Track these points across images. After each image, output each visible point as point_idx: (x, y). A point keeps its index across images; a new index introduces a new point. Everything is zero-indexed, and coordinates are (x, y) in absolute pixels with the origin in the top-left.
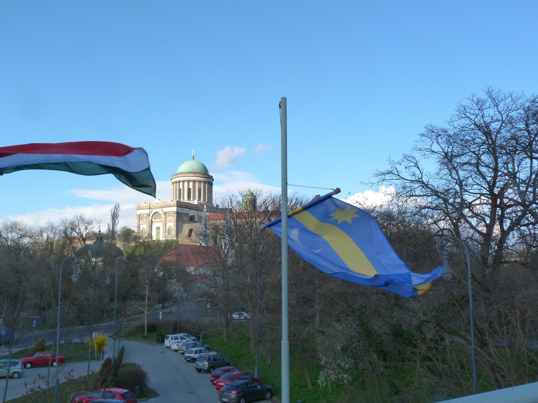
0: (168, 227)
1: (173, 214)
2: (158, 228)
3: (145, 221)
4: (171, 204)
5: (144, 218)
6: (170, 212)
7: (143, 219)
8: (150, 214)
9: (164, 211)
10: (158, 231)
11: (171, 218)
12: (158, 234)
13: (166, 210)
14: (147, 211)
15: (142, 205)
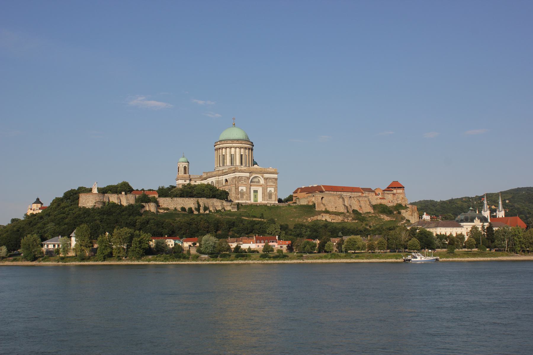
0: (268, 191)
1: (274, 180)
2: (256, 192)
3: (245, 183)
4: (272, 171)
5: (242, 180)
6: (270, 178)
7: (242, 181)
8: (250, 178)
9: (265, 177)
10: (256, 194)
11: (271, 184)
12: (256, 197)
13: (266, 176)
14: (248, 175)
15: (240, 169)
